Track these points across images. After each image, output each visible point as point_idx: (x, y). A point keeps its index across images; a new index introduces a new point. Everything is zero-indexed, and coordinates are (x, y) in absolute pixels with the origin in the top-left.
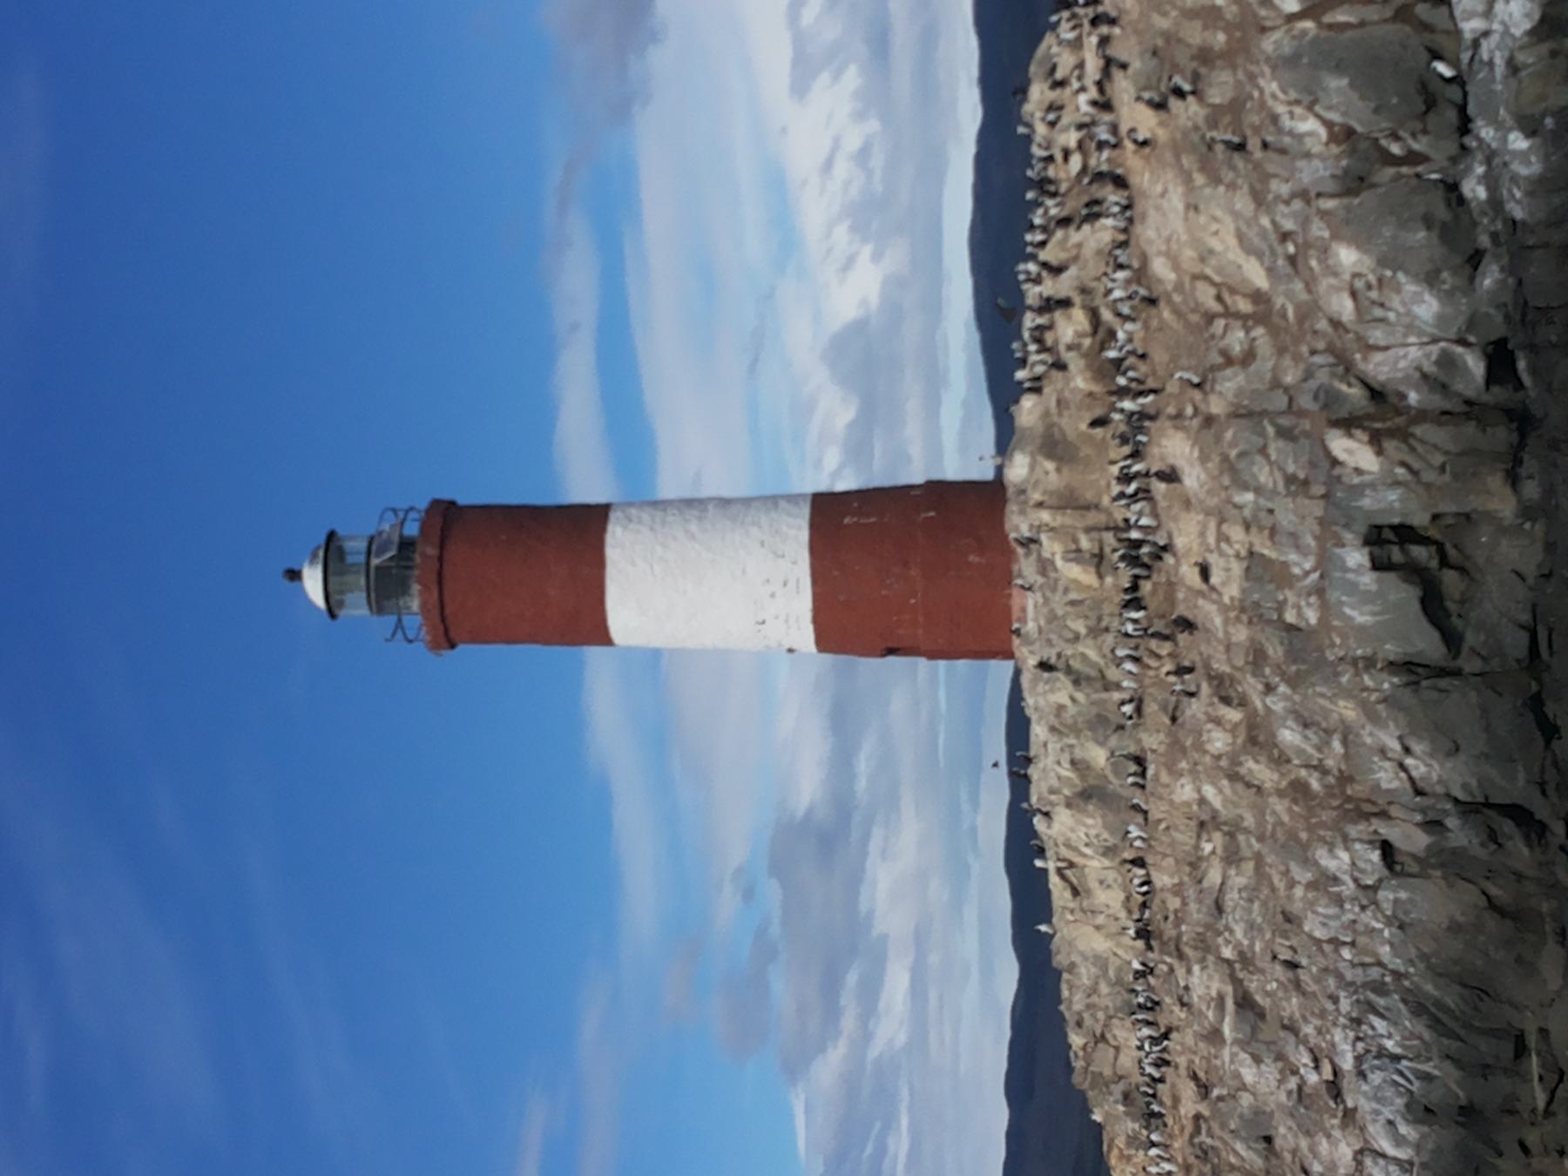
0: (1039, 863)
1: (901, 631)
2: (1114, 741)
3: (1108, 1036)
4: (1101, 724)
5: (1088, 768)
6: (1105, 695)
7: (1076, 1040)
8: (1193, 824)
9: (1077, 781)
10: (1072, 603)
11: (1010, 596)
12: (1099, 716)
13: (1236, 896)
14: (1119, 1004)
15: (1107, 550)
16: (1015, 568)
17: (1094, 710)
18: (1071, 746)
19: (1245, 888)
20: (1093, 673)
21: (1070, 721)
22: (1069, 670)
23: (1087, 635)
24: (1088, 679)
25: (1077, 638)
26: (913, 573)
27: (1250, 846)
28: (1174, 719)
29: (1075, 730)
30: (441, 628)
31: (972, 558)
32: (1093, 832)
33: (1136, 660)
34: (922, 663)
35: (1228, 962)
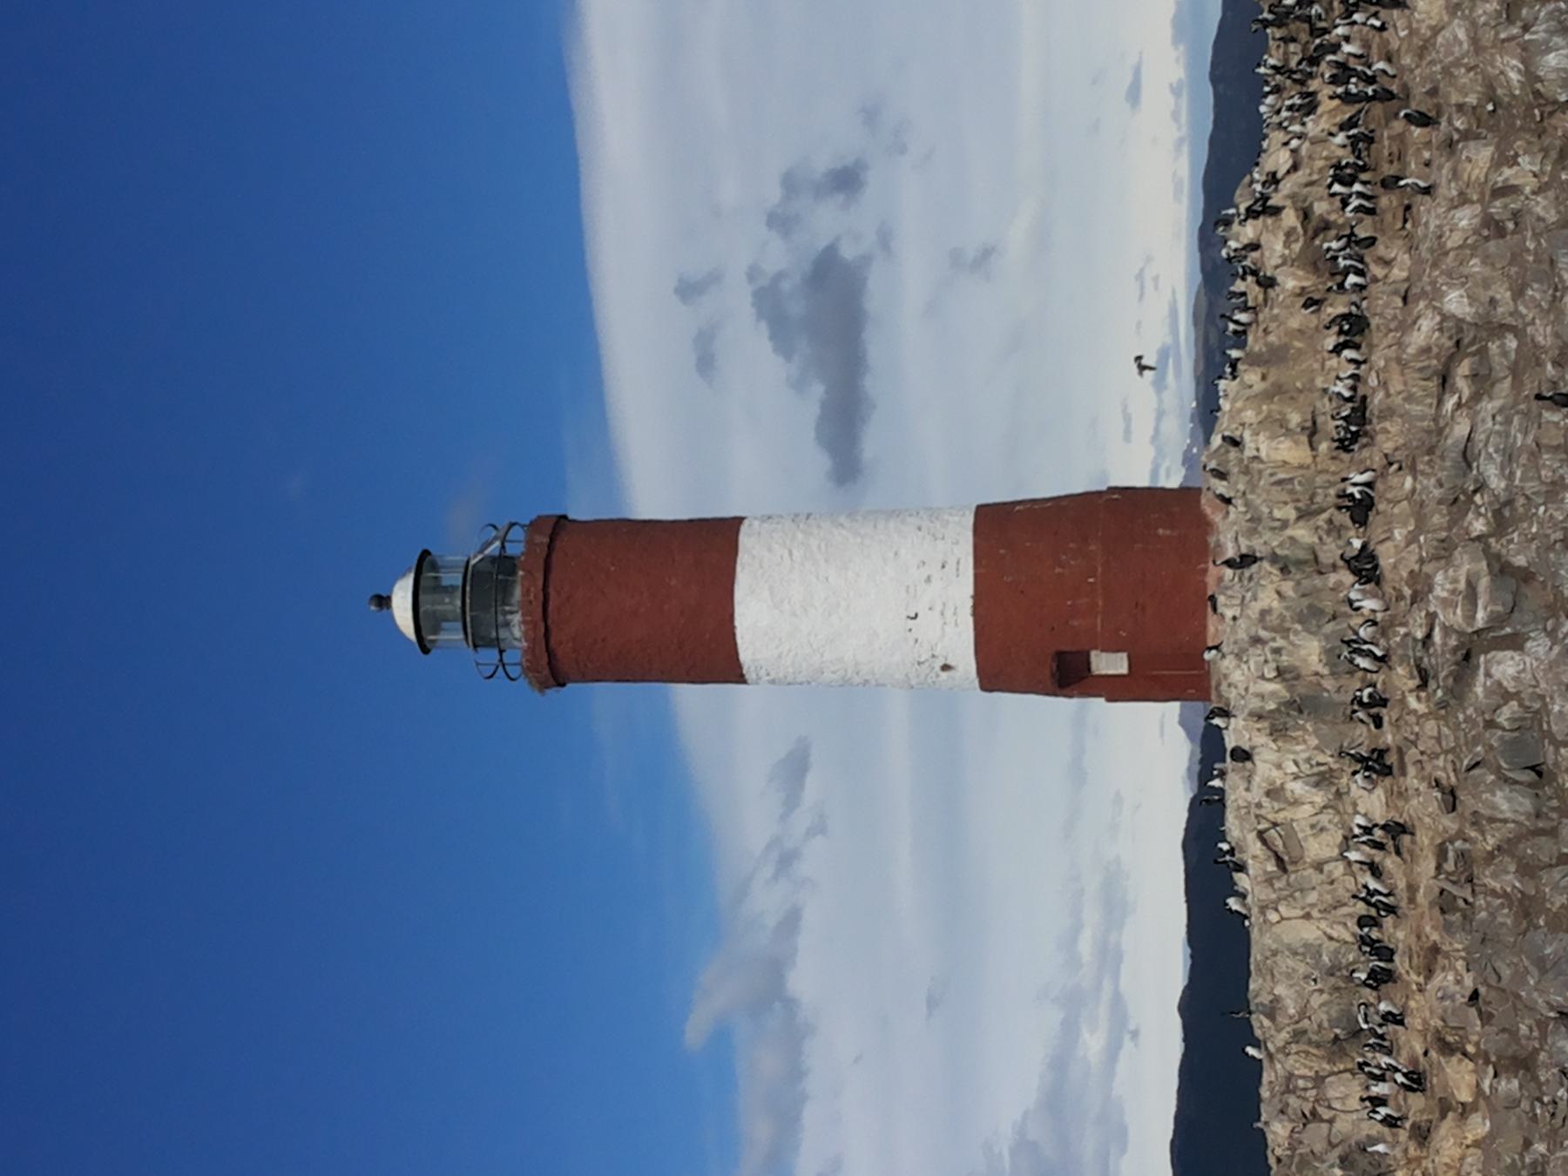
0: (1233, 903)
1: (1076, 623)
2: (1329, 628)
3: (1320, 1110)
4: (1311, 616)
5: (1297, 677)
6: (1317, 581)
7: (1278, 1132)
8: (1433, 385)
9: (1286, 694)
10: (1280, 483)
11: (1205, 571)
12: (1310, 606)
13: (1490, 424)
14: (1334, 1014)
15: (1320, 420)
16: (1212, 540)
17: (1305, 602)
18: (1277, 651)
19: (1501, 410)
20: (1302, 555)
21: (1276, 622)
22: (1274, 558)
23: (1299, 518)
24: (1300, 563)
25: (1285, 524)
26: (1093, 547)
27: (1505, 354)
28: (1405, 299)
29: (1284, 632)
30: (542, 625)
31: (1161, 531)
32: (1305, 755)
33: (1360, 273)
34: (1099, 703)
35: (1479, 538)
